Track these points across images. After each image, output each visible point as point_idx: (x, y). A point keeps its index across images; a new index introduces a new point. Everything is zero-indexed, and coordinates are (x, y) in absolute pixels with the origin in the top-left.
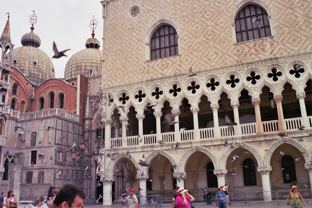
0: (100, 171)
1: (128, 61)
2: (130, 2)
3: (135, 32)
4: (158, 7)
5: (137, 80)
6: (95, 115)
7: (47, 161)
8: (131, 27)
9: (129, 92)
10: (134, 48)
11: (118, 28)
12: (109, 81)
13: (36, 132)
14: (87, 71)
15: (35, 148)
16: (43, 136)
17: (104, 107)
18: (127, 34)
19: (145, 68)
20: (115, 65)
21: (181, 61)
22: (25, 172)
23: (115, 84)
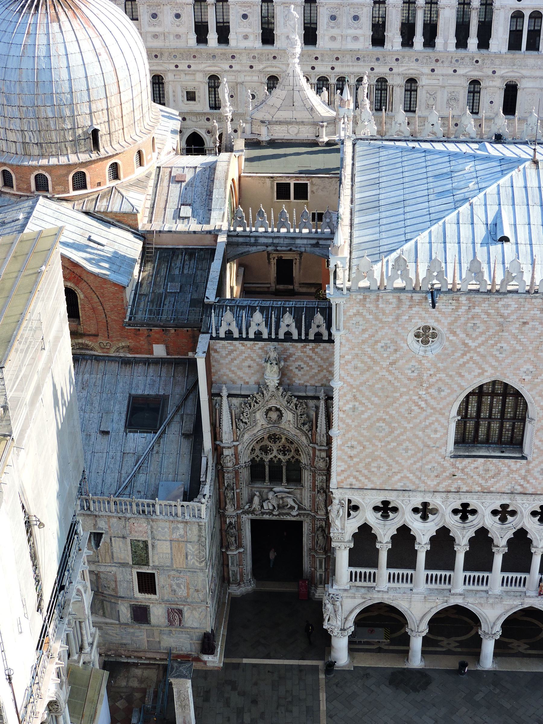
1: (404, 445)
2: (417, 313)
3: (426, 390)
4: (493, 346)
5: (422, 489)
7: (188, 593)
8: (415, 374)
10: (421, 422)
11: (378, 368)
13: (145, 543)
16: (169, 551)
18: (405, 390)
19: (445, 470)
20: (368, 448)
21: (528, 471)
22: (126, 605)
23: (366, 485)
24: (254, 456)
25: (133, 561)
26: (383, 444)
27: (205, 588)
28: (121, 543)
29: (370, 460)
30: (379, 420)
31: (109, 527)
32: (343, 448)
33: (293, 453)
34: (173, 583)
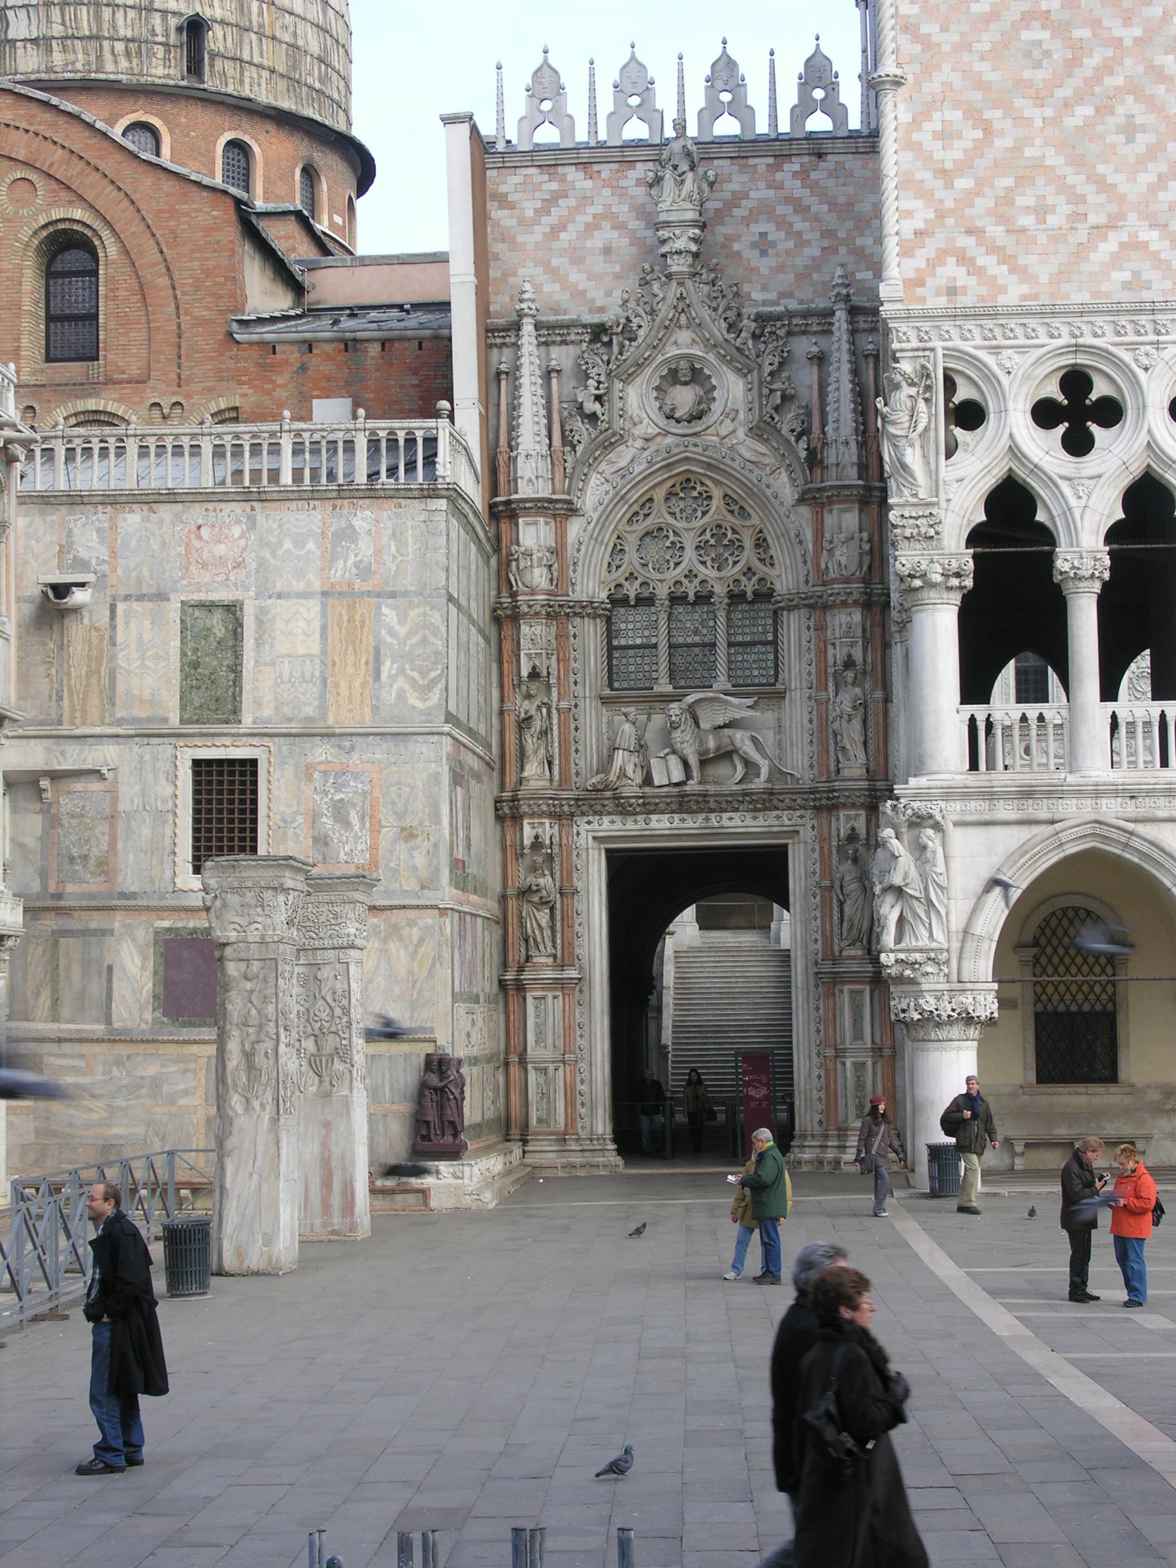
0: (907, 943)
6: (594, 480)
7: (374, 848)
9: (1134, 366)
12: (952, 261)
13: (232, 609)
14: (157, 19)
15: (239, 735)
16: (316, 648)
17: (913, 457)
20: (1002, 133)
22: (143, 934)
23: (1003, 289)
24: (619, 575)
25: (183, 708)
26: (1049, 112)
27: (436, 817)
28: (147, 624)
29: (1009, 182)
30: (1027, 18)
31: (113, 554)
32: (916, 137)
33: (749, 555)
34: (323, 803)
